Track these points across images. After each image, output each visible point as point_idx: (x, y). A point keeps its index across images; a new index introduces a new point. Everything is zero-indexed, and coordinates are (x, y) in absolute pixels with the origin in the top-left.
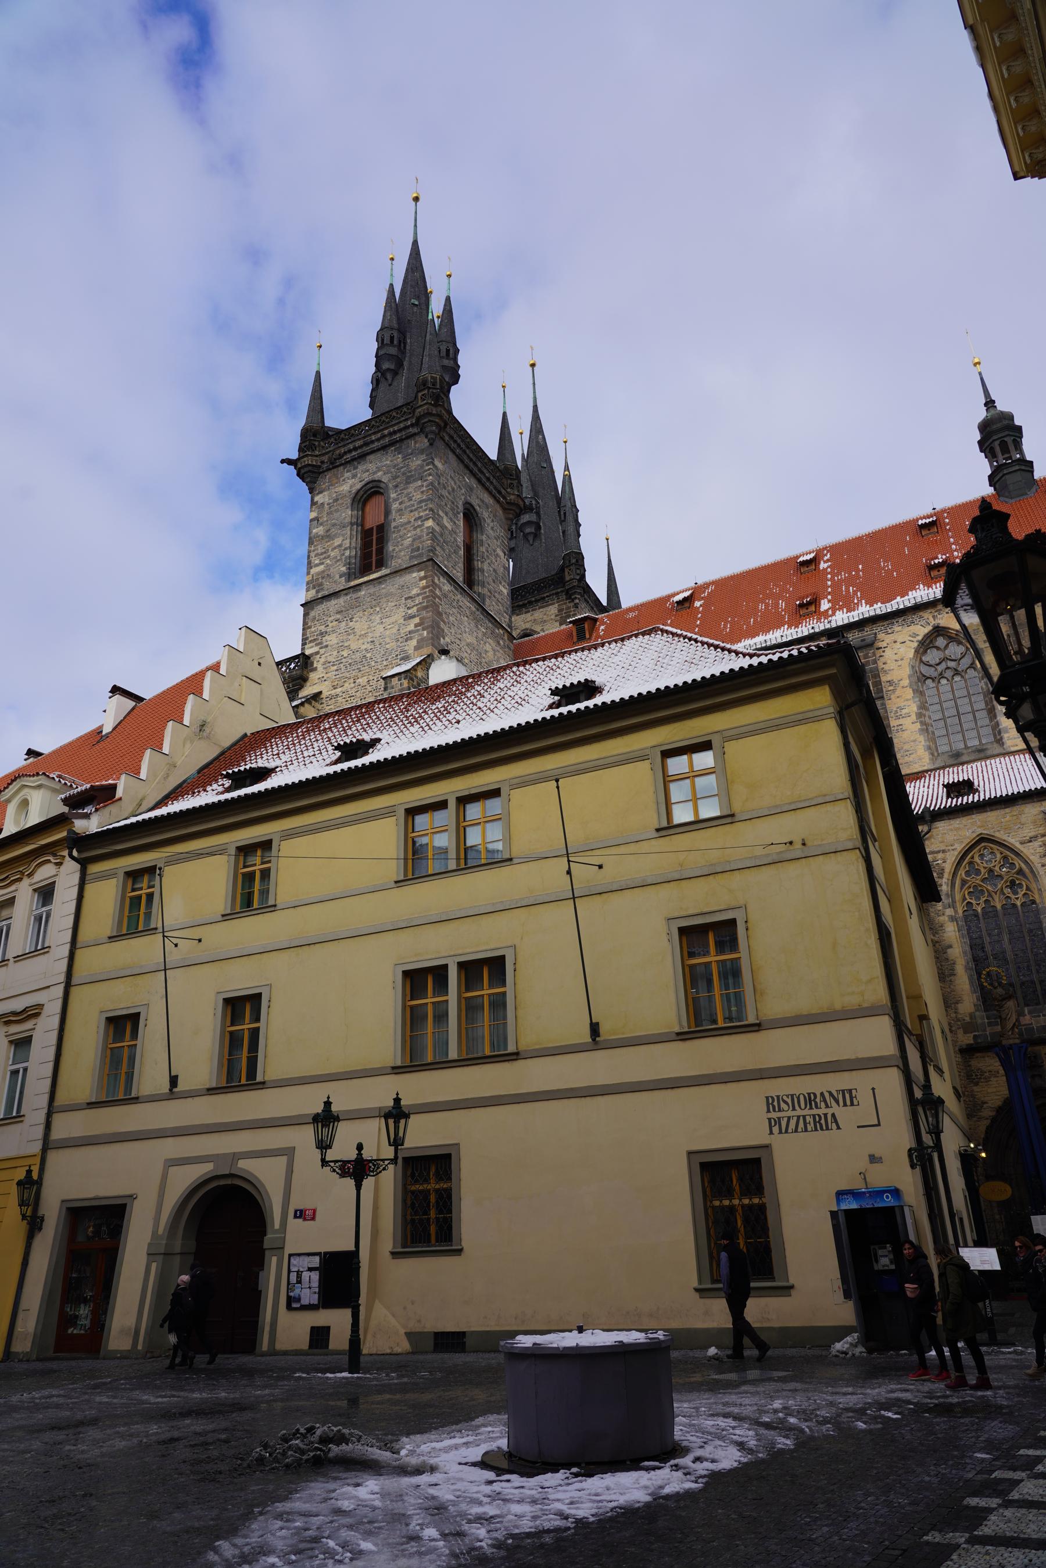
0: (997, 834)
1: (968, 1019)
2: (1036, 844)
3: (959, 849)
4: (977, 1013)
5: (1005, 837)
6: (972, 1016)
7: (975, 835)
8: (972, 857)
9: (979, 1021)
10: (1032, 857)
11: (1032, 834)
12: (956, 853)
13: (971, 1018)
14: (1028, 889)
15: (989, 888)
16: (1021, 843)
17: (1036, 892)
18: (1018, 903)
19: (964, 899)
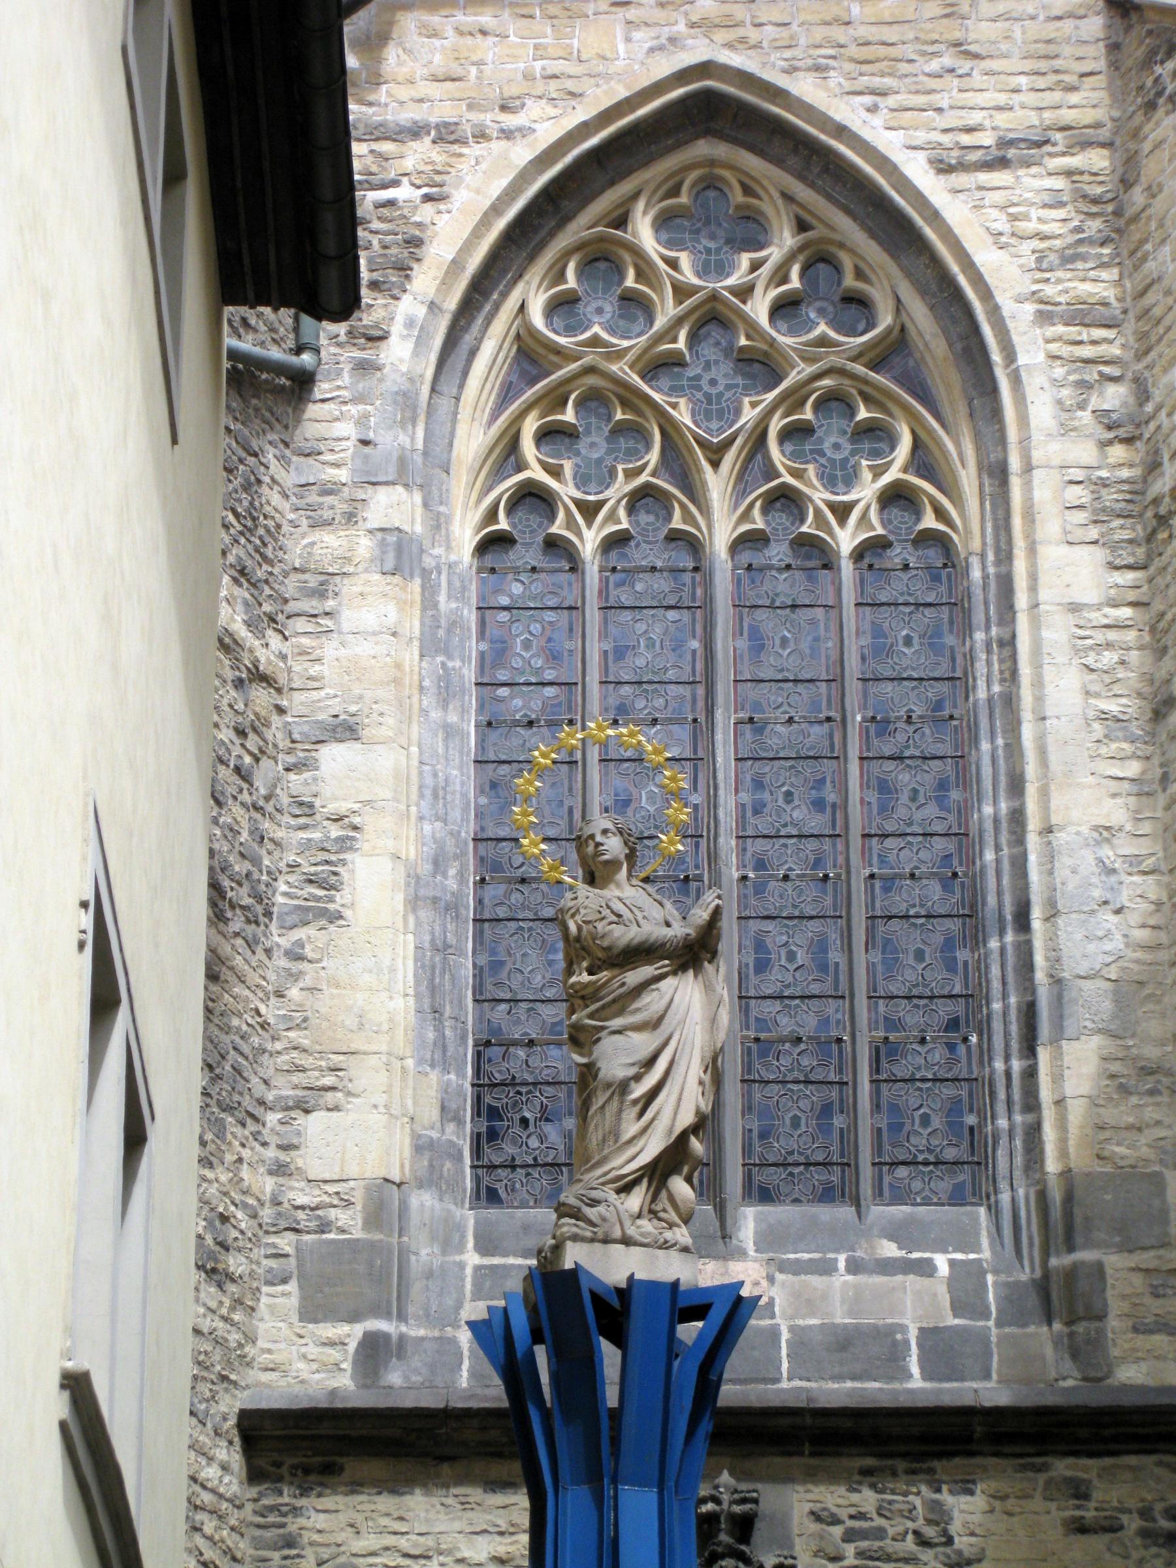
0: (804, 87)
1: (350, 1222)
2: (1032, 183)
3: (548, 133)
4: (423, 1201)
5: (848, 112)
6: (384, 1202)
7: (664, 67)
8: (621, 222)
9: (425, 1253)
10: (986, 257)
11: (1021, 119)
12: (523, 154)
13: (375, 1216)
14: (924, 460)
15: (683, 415)
16: (943, 168)
17: (968, 479)
18: (846, 540)
19: (508, 453)
